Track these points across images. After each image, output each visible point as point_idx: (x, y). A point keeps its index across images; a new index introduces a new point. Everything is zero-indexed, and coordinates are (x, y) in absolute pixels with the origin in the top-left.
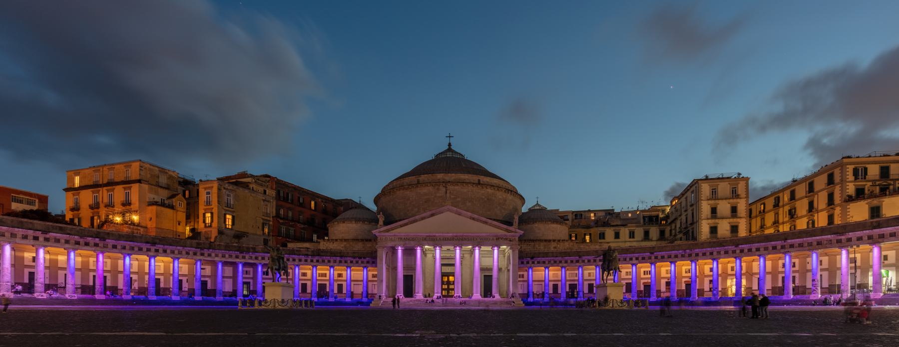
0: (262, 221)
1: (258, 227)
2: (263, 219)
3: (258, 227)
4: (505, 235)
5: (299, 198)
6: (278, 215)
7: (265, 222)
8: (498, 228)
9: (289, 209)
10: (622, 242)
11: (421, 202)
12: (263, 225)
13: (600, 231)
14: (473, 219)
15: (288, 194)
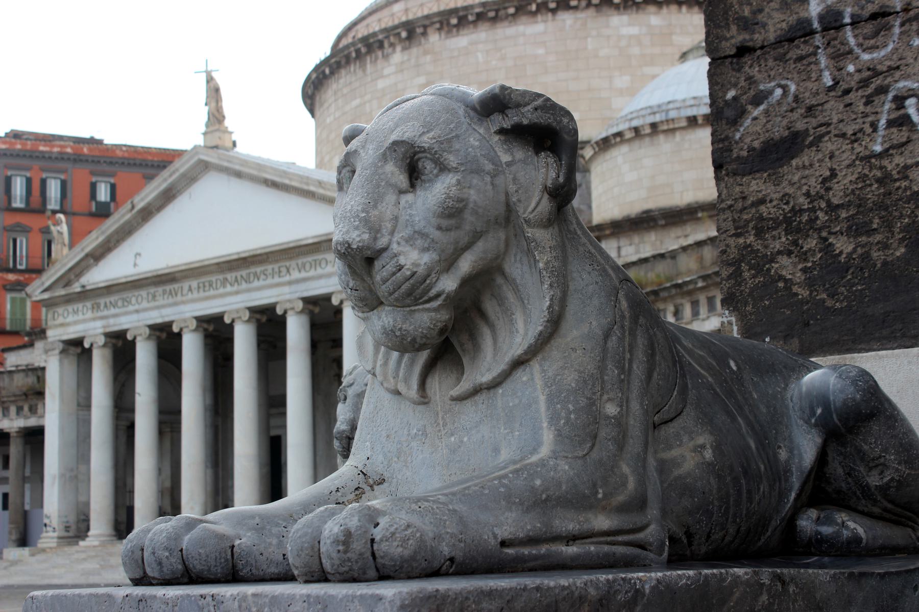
5: (93, 187)
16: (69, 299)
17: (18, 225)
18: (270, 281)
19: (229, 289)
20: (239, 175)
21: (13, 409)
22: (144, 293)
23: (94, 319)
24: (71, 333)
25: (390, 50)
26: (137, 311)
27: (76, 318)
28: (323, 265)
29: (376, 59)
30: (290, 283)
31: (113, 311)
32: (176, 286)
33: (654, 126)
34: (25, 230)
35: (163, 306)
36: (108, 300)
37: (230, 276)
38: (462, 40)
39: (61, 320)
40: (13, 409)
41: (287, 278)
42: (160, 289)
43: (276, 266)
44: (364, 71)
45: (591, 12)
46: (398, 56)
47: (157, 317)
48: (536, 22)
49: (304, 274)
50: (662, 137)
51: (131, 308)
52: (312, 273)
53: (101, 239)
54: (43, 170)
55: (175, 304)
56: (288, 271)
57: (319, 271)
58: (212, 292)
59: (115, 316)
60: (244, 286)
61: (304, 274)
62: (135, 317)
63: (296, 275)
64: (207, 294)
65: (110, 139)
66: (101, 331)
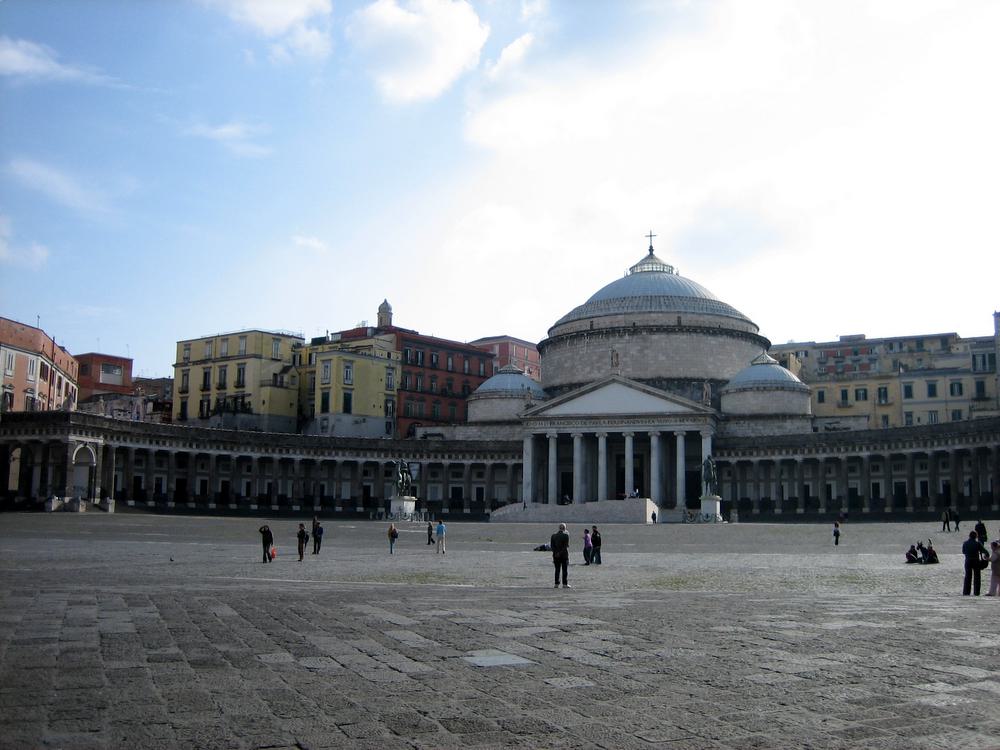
4: (691, 415)
6: (403, 387)
7: (389, 398)
9: (419, 375)
11: (595, 358)
12: (387, 401)
14: (649, 393)
15: (417, 353)
16: (539, 419)
20: (630, 386)
21: (489, 456)
33: (765, 388)
34: (410, 373)
37: (626, 421)
38: (655, 337)
40: (489, 456)
42: (588, 421)
44: (608, 338)
45: (701, 335)
47: (586, 430)
63: (656, 423)
65: (422, 332)
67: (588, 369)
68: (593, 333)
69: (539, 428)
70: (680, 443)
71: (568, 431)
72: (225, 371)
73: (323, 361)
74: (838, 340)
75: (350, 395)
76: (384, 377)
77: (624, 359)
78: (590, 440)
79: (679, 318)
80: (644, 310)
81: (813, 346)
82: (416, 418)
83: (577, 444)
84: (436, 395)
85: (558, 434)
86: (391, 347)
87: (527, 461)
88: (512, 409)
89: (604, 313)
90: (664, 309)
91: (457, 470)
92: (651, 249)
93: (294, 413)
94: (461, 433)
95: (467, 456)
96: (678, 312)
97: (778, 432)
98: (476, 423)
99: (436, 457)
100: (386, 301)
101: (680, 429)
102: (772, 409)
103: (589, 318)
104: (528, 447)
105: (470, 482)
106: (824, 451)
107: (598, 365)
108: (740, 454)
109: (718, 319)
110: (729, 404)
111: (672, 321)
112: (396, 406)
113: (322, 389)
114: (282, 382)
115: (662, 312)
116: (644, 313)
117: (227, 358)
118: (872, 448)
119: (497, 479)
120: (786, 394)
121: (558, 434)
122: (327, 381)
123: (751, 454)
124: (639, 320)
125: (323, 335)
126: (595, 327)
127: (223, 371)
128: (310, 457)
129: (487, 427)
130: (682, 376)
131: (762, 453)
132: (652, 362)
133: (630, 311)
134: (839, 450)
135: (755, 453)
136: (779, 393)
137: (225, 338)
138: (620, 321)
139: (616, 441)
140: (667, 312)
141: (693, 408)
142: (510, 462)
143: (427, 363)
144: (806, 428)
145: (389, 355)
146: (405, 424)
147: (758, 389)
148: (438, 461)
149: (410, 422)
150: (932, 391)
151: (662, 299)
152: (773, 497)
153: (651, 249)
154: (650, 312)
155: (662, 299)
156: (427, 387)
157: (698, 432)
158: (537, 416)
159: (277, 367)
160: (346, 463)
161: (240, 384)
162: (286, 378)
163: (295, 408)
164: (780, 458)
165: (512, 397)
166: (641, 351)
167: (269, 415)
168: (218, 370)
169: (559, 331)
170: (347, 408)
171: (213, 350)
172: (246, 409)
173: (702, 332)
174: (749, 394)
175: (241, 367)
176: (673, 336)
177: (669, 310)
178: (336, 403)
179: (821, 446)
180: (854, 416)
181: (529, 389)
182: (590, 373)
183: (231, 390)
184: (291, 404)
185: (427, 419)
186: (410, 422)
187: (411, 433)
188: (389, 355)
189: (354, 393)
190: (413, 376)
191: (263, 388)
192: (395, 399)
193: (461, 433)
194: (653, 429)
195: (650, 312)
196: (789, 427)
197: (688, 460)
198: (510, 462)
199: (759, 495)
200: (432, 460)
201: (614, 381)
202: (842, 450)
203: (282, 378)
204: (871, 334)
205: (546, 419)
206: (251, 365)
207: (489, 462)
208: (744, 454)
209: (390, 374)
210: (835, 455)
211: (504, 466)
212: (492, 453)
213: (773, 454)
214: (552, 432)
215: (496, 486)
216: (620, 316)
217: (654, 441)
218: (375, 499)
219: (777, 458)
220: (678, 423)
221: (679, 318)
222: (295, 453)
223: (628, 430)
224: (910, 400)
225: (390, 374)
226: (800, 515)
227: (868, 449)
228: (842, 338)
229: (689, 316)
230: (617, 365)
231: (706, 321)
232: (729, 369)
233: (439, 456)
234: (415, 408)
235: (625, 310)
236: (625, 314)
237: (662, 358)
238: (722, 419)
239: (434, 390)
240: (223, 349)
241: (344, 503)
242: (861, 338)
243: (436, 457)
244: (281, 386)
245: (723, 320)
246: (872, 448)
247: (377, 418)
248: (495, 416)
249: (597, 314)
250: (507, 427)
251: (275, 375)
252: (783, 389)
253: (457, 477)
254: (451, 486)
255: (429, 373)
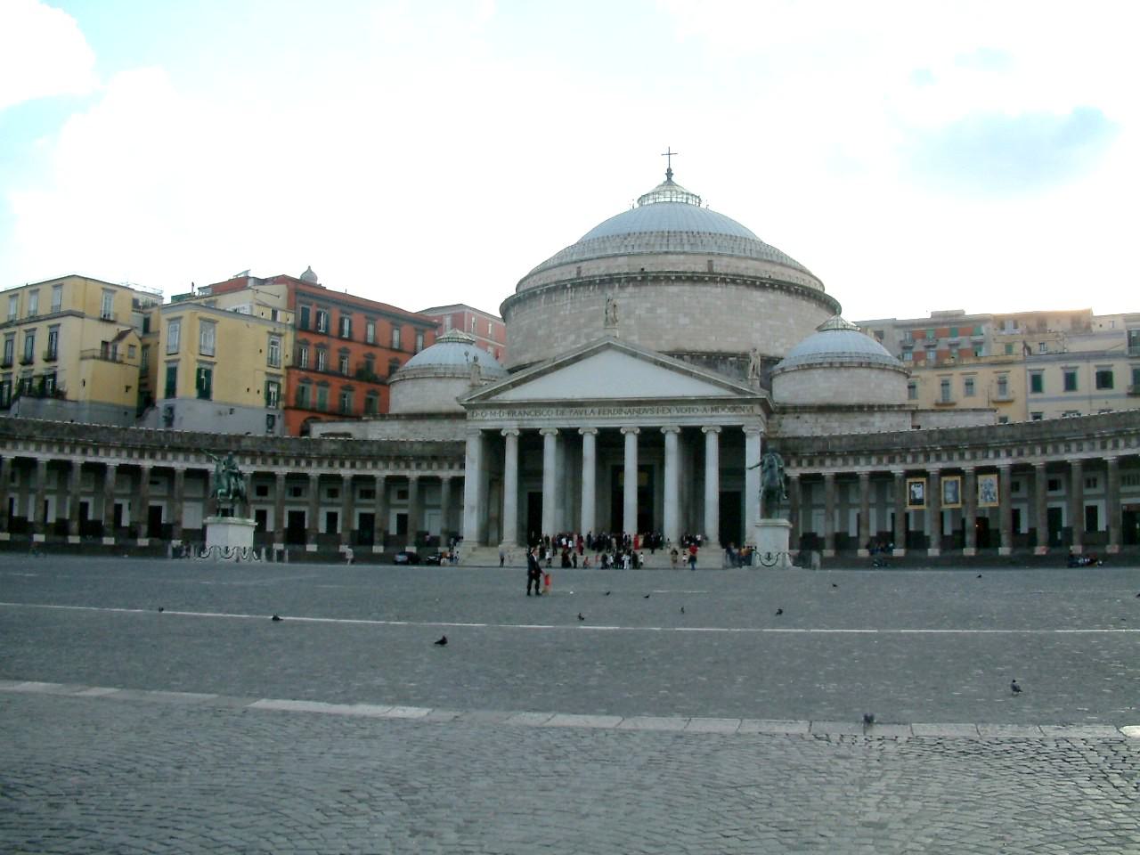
0: (265, 378)
1: (258, 392)
2: (267, 373)
3: (258, 392)
6: (296, 365)
7: (272, 379)
8: (716, 383)
9: (321, 346)
10: (1083, 398)
11: (582, 321)
12: (269, 383)
13: (1030, 370)
14: (663, 365)
17: (305, 340)
18: (655, 414)
19: (624, 415)
20: (634, 355)
22: (554, 410)
23: (511, 420)
24: (490, 425)
25: (626, 284)
26: (549, 419)
27: (493, 417)
28: (693, 411)
29: (613, 287)
30: (671, 417)
31: (526, 416)
32: (581, 409)
33: (842, 363)
34: (307, 343)
35: (571, 419)
36: (522, 410)
37: (625, 409)
38: (673, 289)
39: (479, 417)
41: (669, 414)
42: (568, 409)
43: (661, 408)
44: (603, 292)
46: (630, 289)
47: (565, 424)
48: (717, 287)
49: (680, 414)
50: (843, 370)
51: (542, 417)
52: (687, 414)
53: (524, 376)
54: (318, 306)
55: (581, 419)
56: (670, 410)
57: (692, 414)
58: (610, 415)
59: (532, 420)
60: (635, 414)
61: (680, 414)
62: (547, 422)
63: (675, 413)
64: (606, 416)
66: (516, 427)
67: (572, 337)
68: (581, 283)
69: (490, 421)
70: (712, 446)
71: (536, 424)
72: (33, 337)
73: (171, 320)
74: (928, 316)
75: (208, 373)
76: (265, 347)
77: (627, 322)
78: (570, 440)
79: (710, 262)
80: (657, 249)
81: (897, 325)
82: (313, 410)
83: (550, 446)
84: (348, 377)
85: (521, 430)
86: (280, 303)
87: (472, 475)
88: (447, 395)
89: (595, 256)
90: (687, 248)
91: (364, 486)
92: (669, 173)
93: (132, 400)
94: (377, 431)
95: (381, 465)
96: (709, 254)
97: (860, 431)
98: (398, 417)
99: (331, 465)
100: (309, 267)
101: (712, 422)
102: (853, 399)
103: (575, 262)
104: (474, 451)
105: (387, 505)
106: (938, 458)
107: (586, 331)
108: (805, 463)
109: (768, 267)
110: (785, 390)
111: (700, 266)
112: (283, 391)
113: (168, 362)
114: (115, 354)
115: (684, 253)
116: (659, 254)
117: (35, 319)
118: (1015, 453)
119: (428, 502)
120: (874, 375)
121: (521, 430)
122: (174, 351)
123: (822, 463)
124: (650, 265)
125: (186, 290)
126: (583, 275)
127: (31, 335)
128: (132, 462)
129: (415, 422)
130: (714, 348)
131: (840, 461)
132: (669, 326)
133: (636, 250)
134: (962, 457)
135: (828, 462)
136: (864, 372)
137: (34, 289)
138: (621, 266)
139: (610, 442)
140: (694, 254)
141: (733, 389)
142: (446, 474)
143: (334, 329)
144: (904, 424)
145: (274, 313)
146: (298, 418)
147: (831, 365)
148: (336, 472)
149: (307, 415)
150: (1070, 382)
151: (685, 236)
152: (853, 533)
153: (669, 173)
154: (666, 253)
155: (685, 236)
156: (334, 364)
157: (741, 427)
158: (486, 402)
159: (109, 333)
160: (190, 473)
161: (51, 357)
162: (122, 348)
163: (134, 392)
164: (870, 469)
165: (453, 377)
166: (651, 310)
167: (92, 402)
168: (23, 336)
169: (531, 284)
170: (204, 392)
171: (19, 306)
172: (59, 395)
173: (745, 282)
174: (817, 374)
175: (54, 330)
176: (700, 289)
177: (695, 250)
178: (186, 385)
179: (933, 449)
180: (974, 410)
181: (476, 359)
182: (574, 343)
183: (40, 367)
184: (128, 388)
185: (332, 414)
186: (307, 415)
187: (305, 431)
188: (274, 313)
189: (216, 371)
190: (312, 350)
191: (85, 363)
192: (282, 381)
193: (377, 431)
194: (670, 424)
195: (666, 253)
196: (877, 424)
197: (724, 473)
198: (446, 474)
199: (833, 529)
200: (325, 470)
201: (609, 346)
202: (967, 456)
203: (115, 348)
204: (972, 310)
205: (502, 406)
206: (69, 327)
207: (413, 474)
208: (811, 464)
209: (273, 343)
210: (957, 464)
211: (436, 481)
212: (420, 459)
213: (857, 463)
214: (510, 426)
215: (428, 512)
216: (621, 260)
217: (671, 443)
218: (169, 527)
219: (863, 468)
220: (709, 413)
221: (710, 262)
222: (107, 455)
223: (629, 425)
224: (1038, 395)
225: (273, 343)
226: (898, 558)
227: (1009, 454)
228: (934, 315)
229: (725, 260)
230: (615, 321)
231: (750, 268)
232: (784, 341)
233: (337, 464)
234: (313, 395)
235: (630, 250)
236: (629, 255)
237: (683, 320)
238: (771, 410)
239: (345, 372)
240: (31, 305)
241: (46, 527)
242: (960, 314)
243: (331, 465)
244: (114, 360)
245: (777, 269)
246: (1015, 453)
247: (253, 408)
248: (429, 406)
249: (587, 256)
250: (446, 422)
251: (105, 343)
252: (869, 366)
253: (367, 498)
254: (358, 511)
255: (336, 345)
